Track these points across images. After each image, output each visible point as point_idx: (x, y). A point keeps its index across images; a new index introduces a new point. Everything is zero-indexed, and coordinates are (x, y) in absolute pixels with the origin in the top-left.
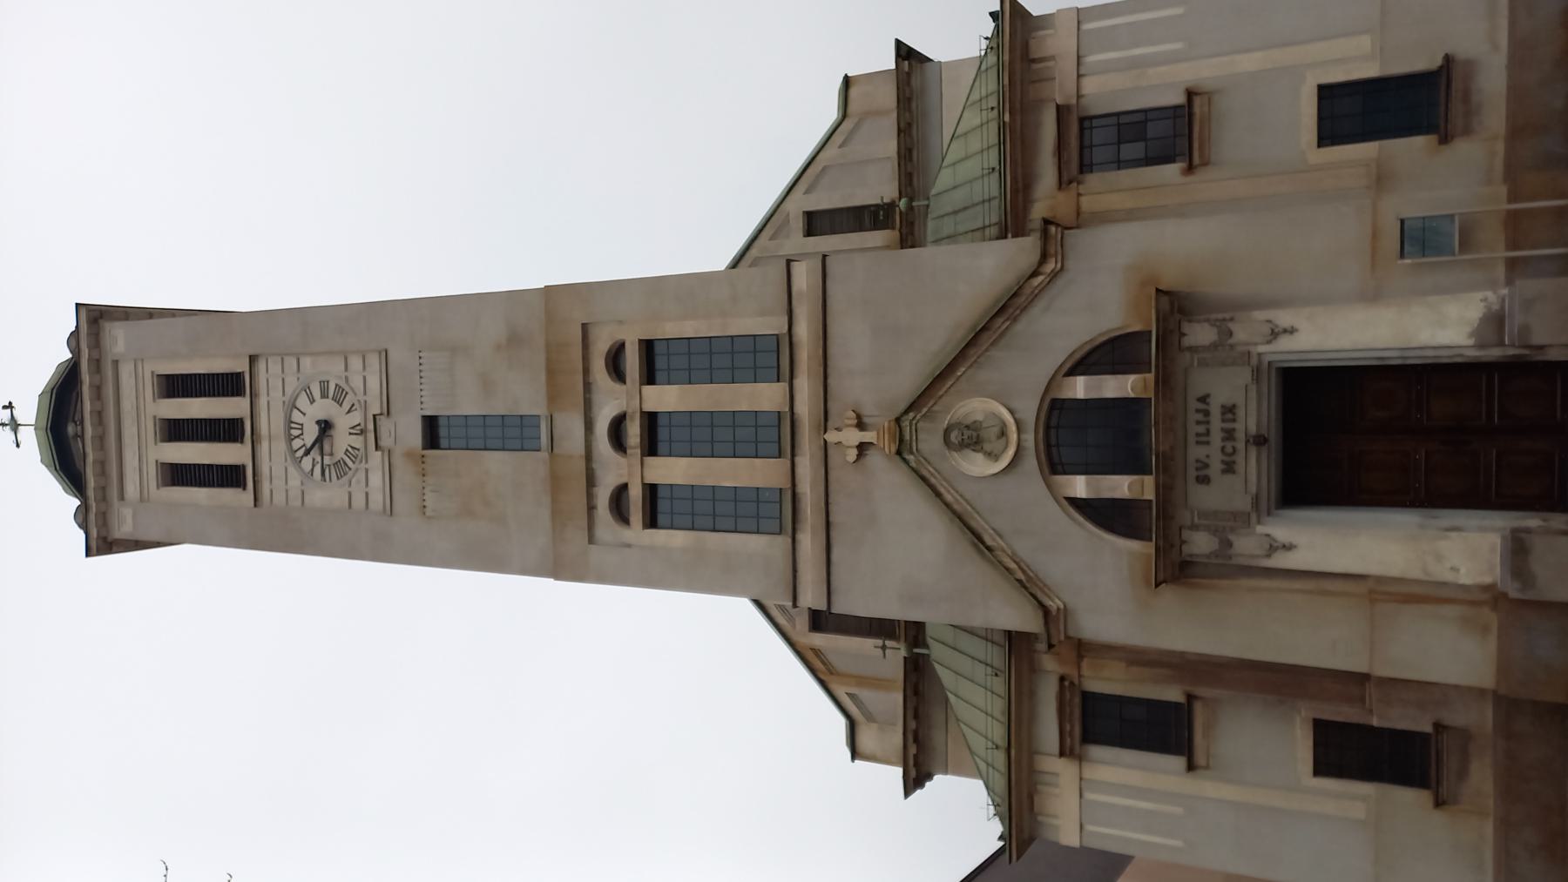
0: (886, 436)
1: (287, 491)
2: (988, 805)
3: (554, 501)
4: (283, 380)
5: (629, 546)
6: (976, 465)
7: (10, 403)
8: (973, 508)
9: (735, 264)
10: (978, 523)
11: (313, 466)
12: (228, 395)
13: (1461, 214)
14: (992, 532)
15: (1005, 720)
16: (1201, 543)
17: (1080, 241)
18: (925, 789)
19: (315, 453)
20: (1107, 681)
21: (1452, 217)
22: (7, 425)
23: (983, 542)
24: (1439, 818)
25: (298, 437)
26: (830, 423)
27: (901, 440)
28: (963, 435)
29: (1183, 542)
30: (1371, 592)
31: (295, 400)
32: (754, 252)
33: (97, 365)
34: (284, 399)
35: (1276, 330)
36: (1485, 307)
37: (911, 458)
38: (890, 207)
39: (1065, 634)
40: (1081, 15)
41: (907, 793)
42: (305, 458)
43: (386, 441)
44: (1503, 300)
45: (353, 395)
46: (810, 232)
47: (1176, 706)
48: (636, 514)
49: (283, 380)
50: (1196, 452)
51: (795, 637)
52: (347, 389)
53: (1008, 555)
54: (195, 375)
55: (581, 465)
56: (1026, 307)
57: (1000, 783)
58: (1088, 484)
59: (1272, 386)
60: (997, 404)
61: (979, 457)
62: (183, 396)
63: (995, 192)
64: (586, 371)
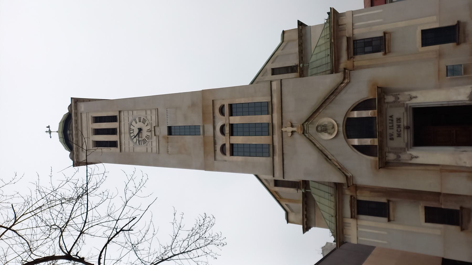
1: (129, 148)
3: (204, 149)
5: (226, 161)
6: (326, 136)
7: (49, 126)
8: (325, 149)
9: (252, 83)
10: (326, 152)
11: (137, 141)
12: (112, 122)
13: (464, 64)
14: (330, 155)
16: (391, 157)
19: (137, 137)
20: (364, 197)
21: (461, 65)
23: (328, 158)
24: (462, 234)
25: (132, 133)
29: (386, 156)
31: (132, 122)
32: (257, 80)
33: (76, 114)
34: (129, 122)
37: (307, 135)
38: (296, 66)
39: (352, 183)
40: (353, 13)
41: (304, 232)
42: (134, 139)
43: (157, 134)
45: (148, 121)
46: (273, 74)
47: (384, 203)
48: (228, 152)
50: (389, 131)
51: (270, 188)
52: (146, 119)
54: (103, 116)
57: (333, 226)
58: (358, 141)
59: (410, 113)
60: (332, 119)
61: (326, 134)
62: (99, 122)
63: (329, 61)
64: (214, 113)
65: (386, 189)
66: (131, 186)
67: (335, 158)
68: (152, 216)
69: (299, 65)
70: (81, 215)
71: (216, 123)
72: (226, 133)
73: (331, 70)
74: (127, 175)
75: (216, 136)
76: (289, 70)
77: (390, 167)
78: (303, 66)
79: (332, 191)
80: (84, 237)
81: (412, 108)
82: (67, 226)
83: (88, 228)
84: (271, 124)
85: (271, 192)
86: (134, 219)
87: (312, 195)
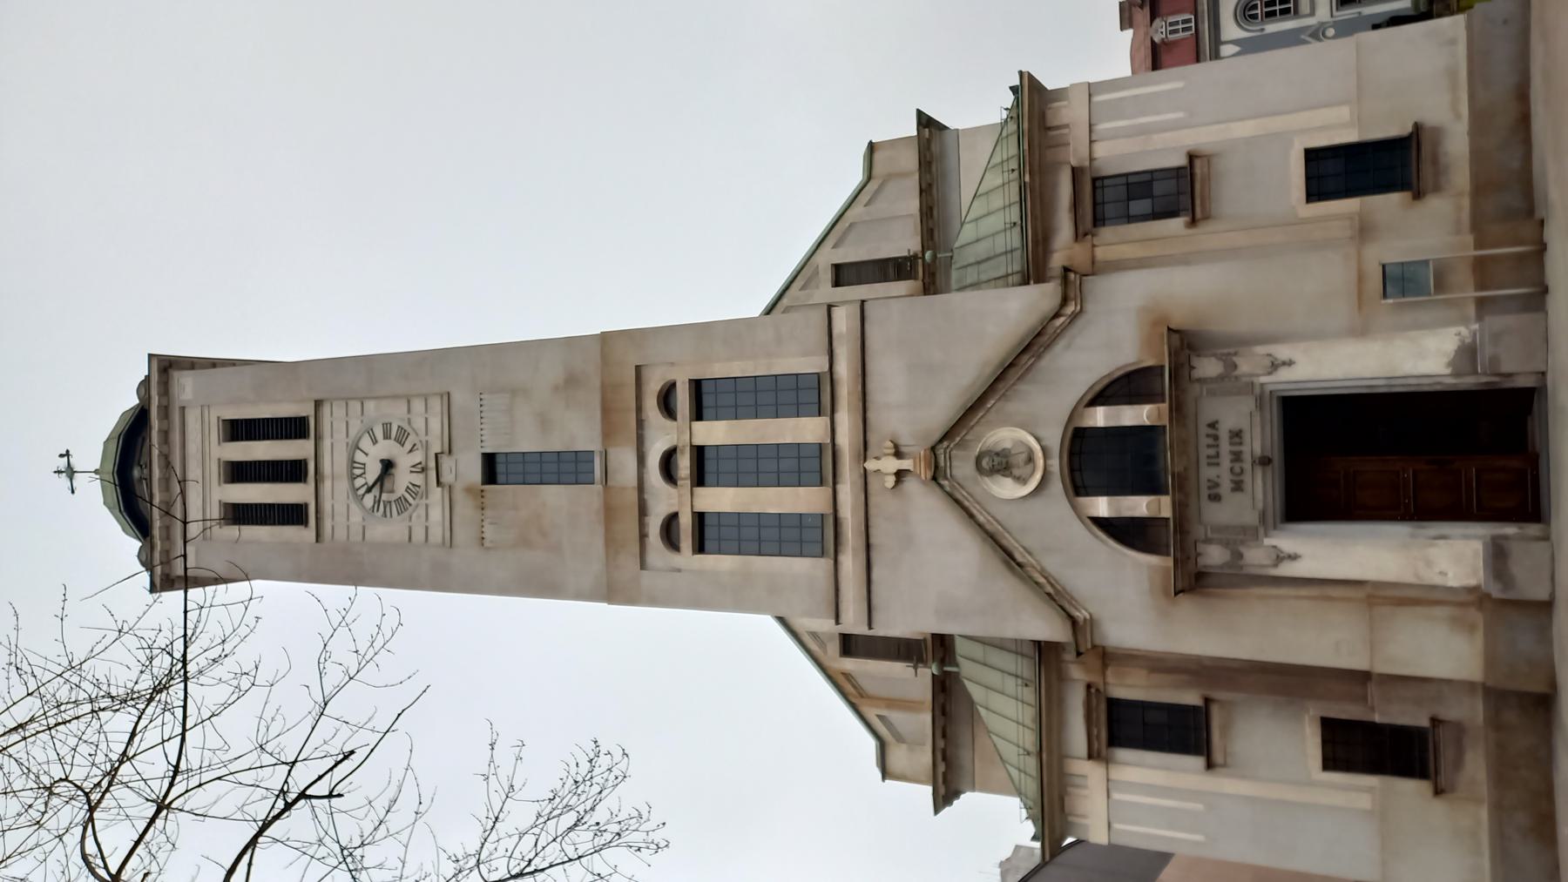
1: (348, 527)
2: (1021, 808)
4: (347, 422)
5: (679, 570)
6: (1005, 489)
7: (68, 451)
9: (769, 311)
10: (1009, 542)
12: (290, 438)
13: (1433, 260)
14: (1021, 549)
15: (1035, 726)
16: (1214, 556)
18: (952, 807)
19: (376, 491)
20: (1130, 687)
21: (1426, 262)
22: (62, 472)
23: (1014, 559)
24: (1439, 807)
25: (360, 476)
26: (869, 453)
27: (936, 467)
28: (993, 461)
29: (1199, 555)
30: (1369, 597)
31: (360, 438)
32: (785, 301)
33: (165, 411)
36: (1460, 340)
37: (945, 483)
40: (1092, 89)
41: (937, 810)
43: (447, 477)
44: (1475, 334)
45: (414, 435)
46: (837, 283)
47: (1194, 708)
48: (686, 541)
49: (347, 422)
50: (1208, 473)
52: (409, 430)
54: (259, 420)
55: (633, 497)
56: (1049, 346)
57: (1032, 787)
58: (1109, 504)
59: (1274, 413)
61: (1008, 481)
64: (639, 409)
66: (341, 649)
67: (1036, 561)
68: (411, 751)
69: (920, 255)
70: (161, 745)
71: (648, 443)
72: (679, 475)
73: (1021, 272)
74: (326, 610)
75: (647, 486)
76: (891, 271)
78: (934, 257)
79: (1026, 668)
80: (172, 823)
81: (1279, 397)
82: (111, 789)
83: (187, 791)
84: (830, 447)
85: (830, 673)
86: (346, 757)
87: (964, 686)
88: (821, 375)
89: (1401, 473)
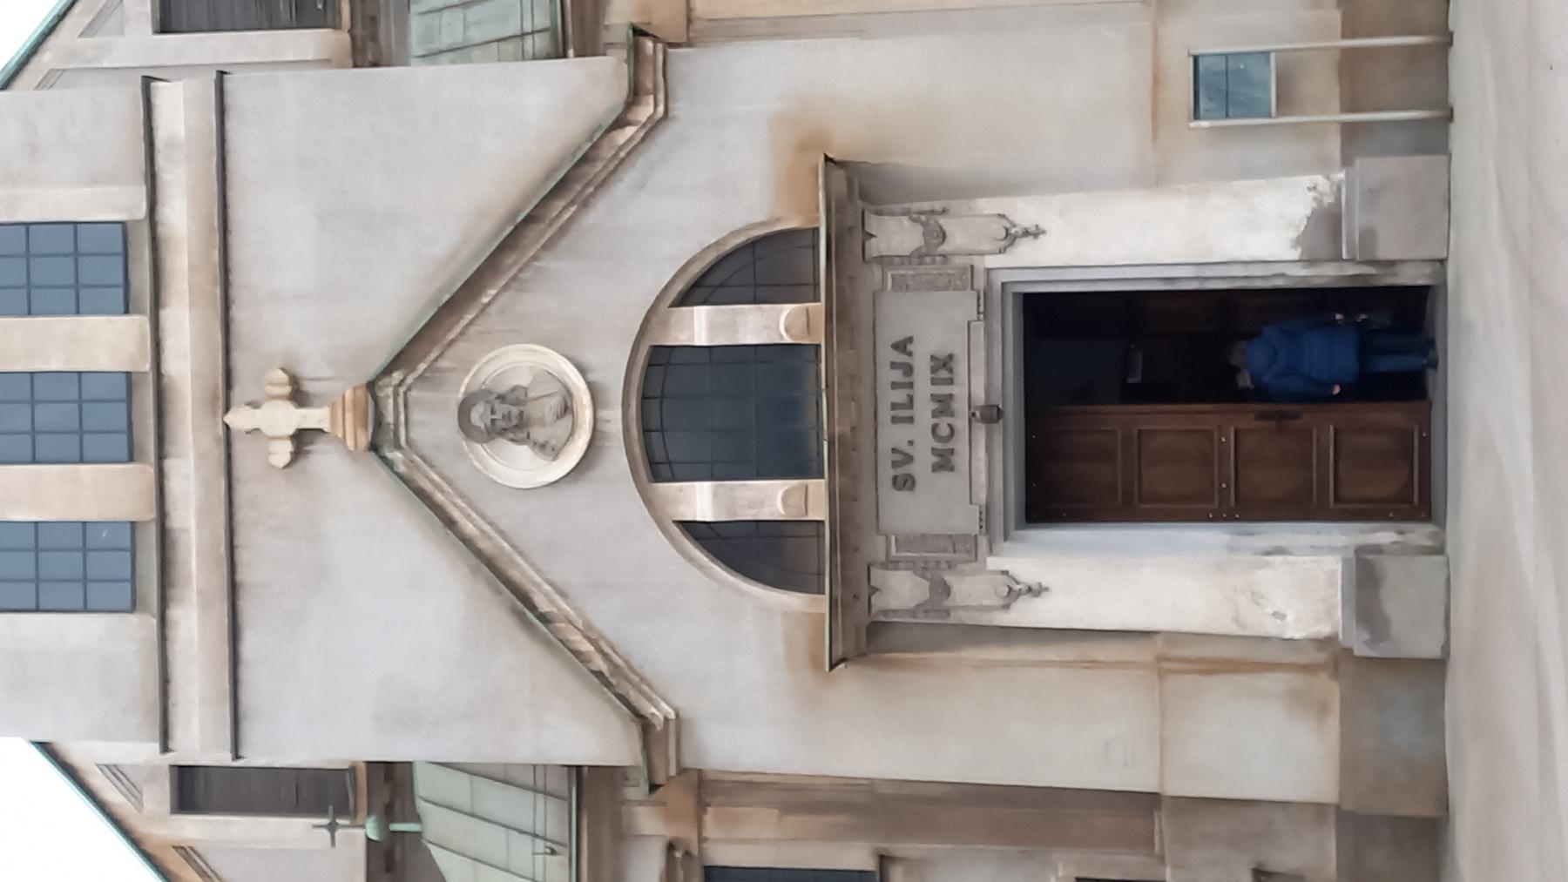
0: (349, 416)
8: (514, 547)
10: (522, 572)
14: (547, 587)
17: (692, 66)
21: (1267, 53)
23: (532, 607)
26: (236, 394)
27: (379, 423)
28: (493, 412)
29: (874, 590)
30: (1161, 659)
35: (1013, 231)
36: (1315, 199)
37: (396, 456)
44: (1339, 189)
50: (892, 436)
53: (578, 629)
56: (604, 183)
58: (715, 495)
59: (1008, 325)
61: (524, 450)
65: (871, 785)
73: (551, 30)
77: (887, 655)
79: (552, 818)
81: (1015, 294)
85: (150, 849)
87: (431, 856)
88: (129, 226)
89: (1216, 438)
